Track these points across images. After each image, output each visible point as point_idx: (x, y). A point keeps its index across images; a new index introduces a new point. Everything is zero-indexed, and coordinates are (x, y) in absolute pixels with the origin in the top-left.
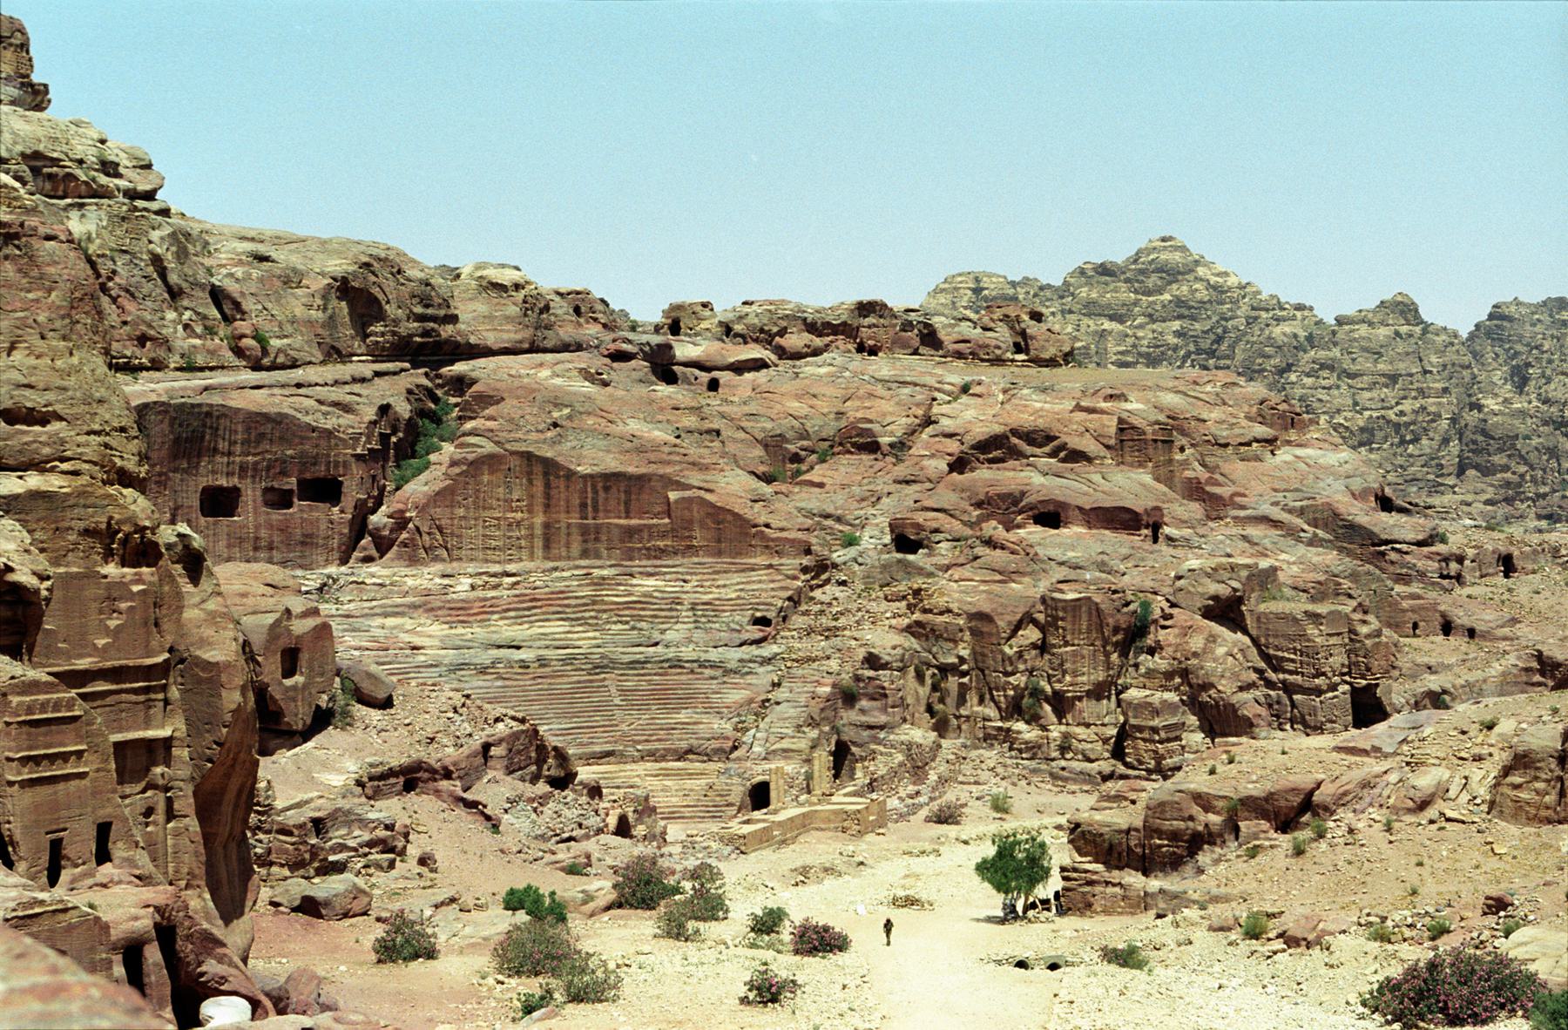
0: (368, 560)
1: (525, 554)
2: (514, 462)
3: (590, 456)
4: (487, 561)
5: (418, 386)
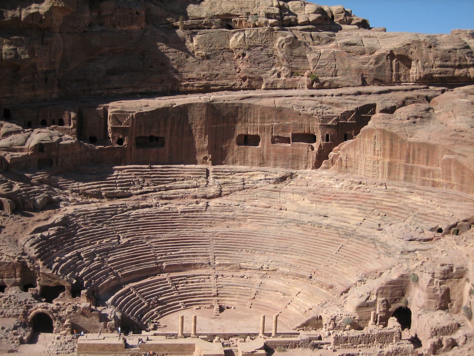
1: (380, 175)
2: (378, 133)
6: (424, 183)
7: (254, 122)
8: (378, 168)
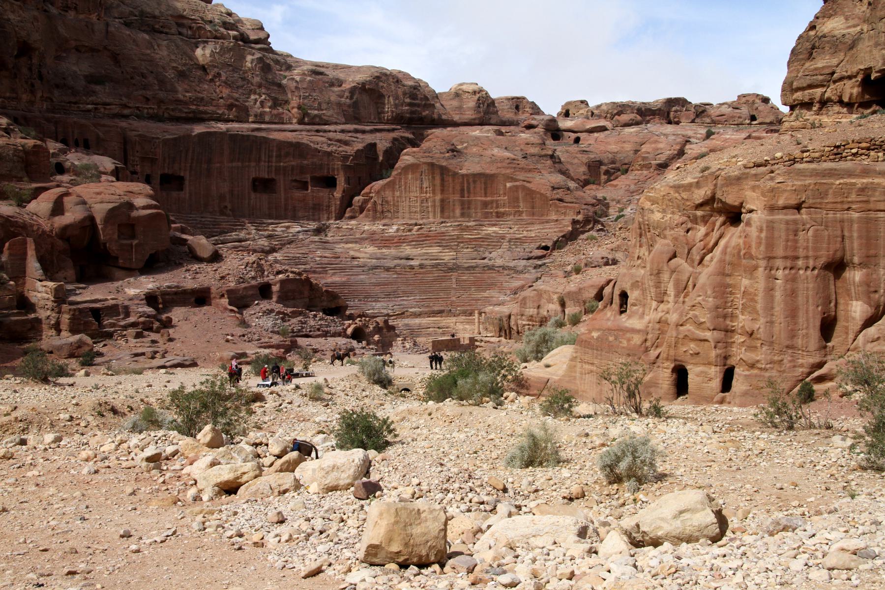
0: (352, 218)
1: (431, 215)
3: (469, 167)
4: (411, 219)
5: (402, 137)
6: (486, 215)
7: (269, 162)
8: (427, 207)
